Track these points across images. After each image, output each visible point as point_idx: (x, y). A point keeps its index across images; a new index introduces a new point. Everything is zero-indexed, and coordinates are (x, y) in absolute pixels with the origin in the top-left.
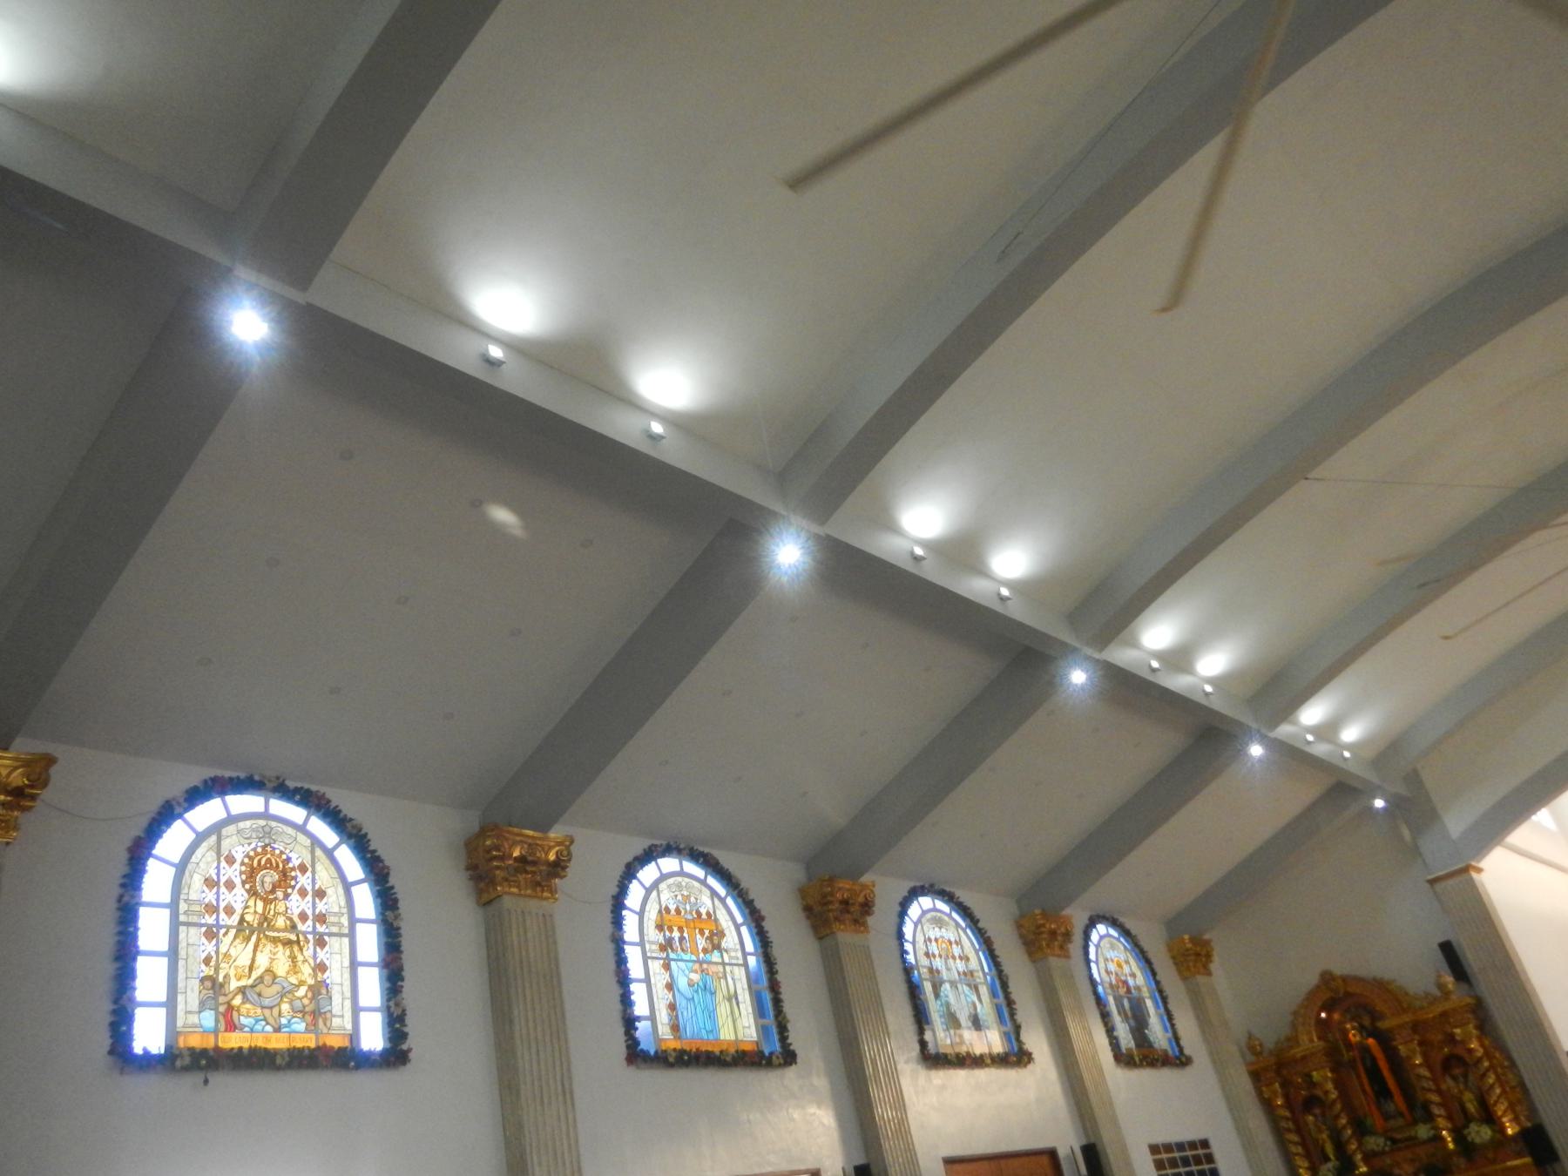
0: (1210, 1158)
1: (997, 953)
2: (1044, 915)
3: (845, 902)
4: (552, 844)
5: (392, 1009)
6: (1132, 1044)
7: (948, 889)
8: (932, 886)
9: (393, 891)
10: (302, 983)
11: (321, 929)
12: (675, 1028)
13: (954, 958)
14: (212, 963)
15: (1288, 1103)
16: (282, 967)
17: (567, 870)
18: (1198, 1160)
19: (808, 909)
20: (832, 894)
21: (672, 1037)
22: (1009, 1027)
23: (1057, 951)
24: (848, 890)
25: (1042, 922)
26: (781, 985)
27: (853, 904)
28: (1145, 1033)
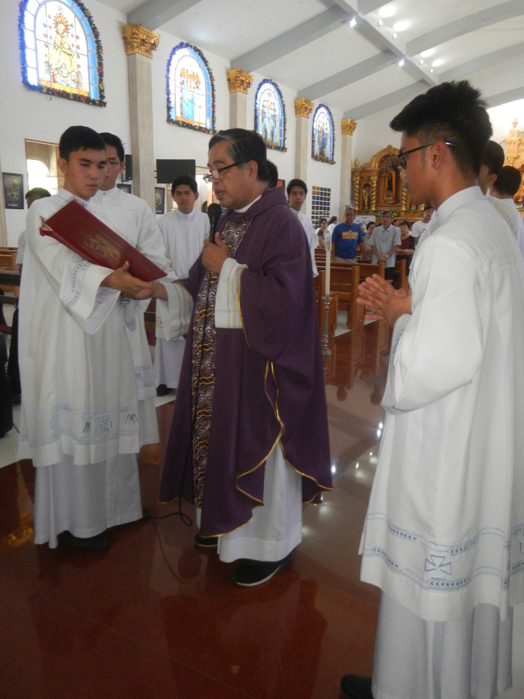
0: (329, 195)
1: (285, 111)
2: (306, 101)
3: (243, 81)
4: (153, 36)
5: (100, 87)
6: (318, 153)
7: (276, 82)
8: (271, 80)
9: (100, 43)
10: (74, 71)
11: (78, 51)
12: (182, 113)
13: (271, 109)
14: (48, 57)
15: (360, 184)
16: (68, 63)
17: (157, 48)
18: (325, 194)
19: (229, 80)
20: (239, 77)
21: (180, 116)
22: (282, 138)
23: (305, 115)
24: (244, 76)
25: (304, 104)
26: (216, 106)
27: (245, 82)
28: (323, 150)
